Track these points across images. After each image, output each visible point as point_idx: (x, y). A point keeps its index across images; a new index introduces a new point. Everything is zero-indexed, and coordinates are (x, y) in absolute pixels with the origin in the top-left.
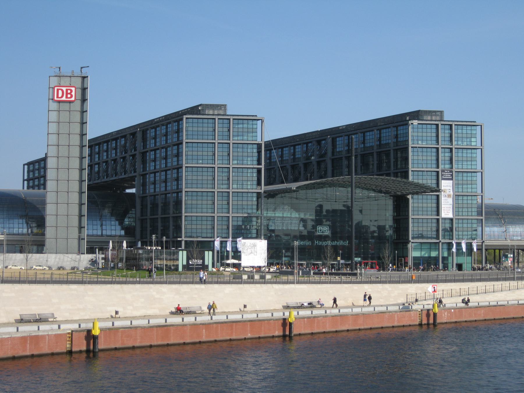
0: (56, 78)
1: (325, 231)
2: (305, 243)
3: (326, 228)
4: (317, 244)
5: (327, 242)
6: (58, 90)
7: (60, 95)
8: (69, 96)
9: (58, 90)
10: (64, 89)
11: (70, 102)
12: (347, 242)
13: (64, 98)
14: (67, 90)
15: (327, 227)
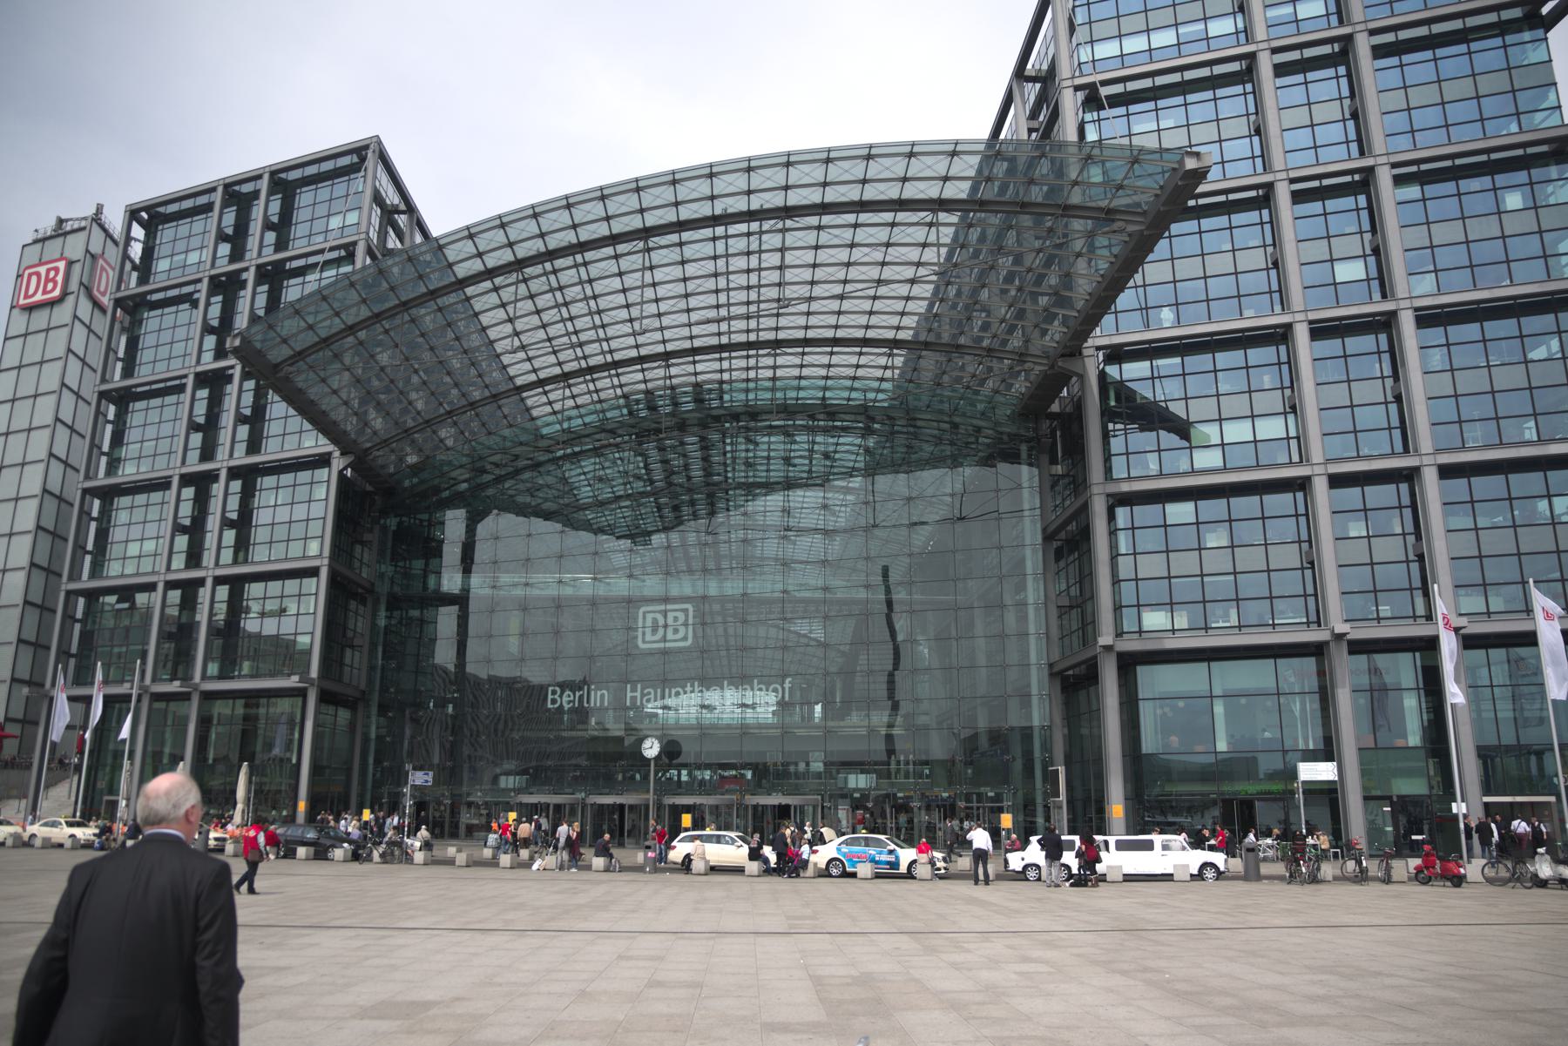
0: (39, 246)
1: (676, 631)
2: (581, 697)
3: (677, 614)
4: (634, 699)
5: (684, 687)
6: (30, 276)
7: (31, 291)
8: (50, 286)
9: (30, 276)
10: (42, 270)
11: (52, 304)
12: (787, 685)
13: (39, 297)
14: (48, 271)
15: (685, 611)
